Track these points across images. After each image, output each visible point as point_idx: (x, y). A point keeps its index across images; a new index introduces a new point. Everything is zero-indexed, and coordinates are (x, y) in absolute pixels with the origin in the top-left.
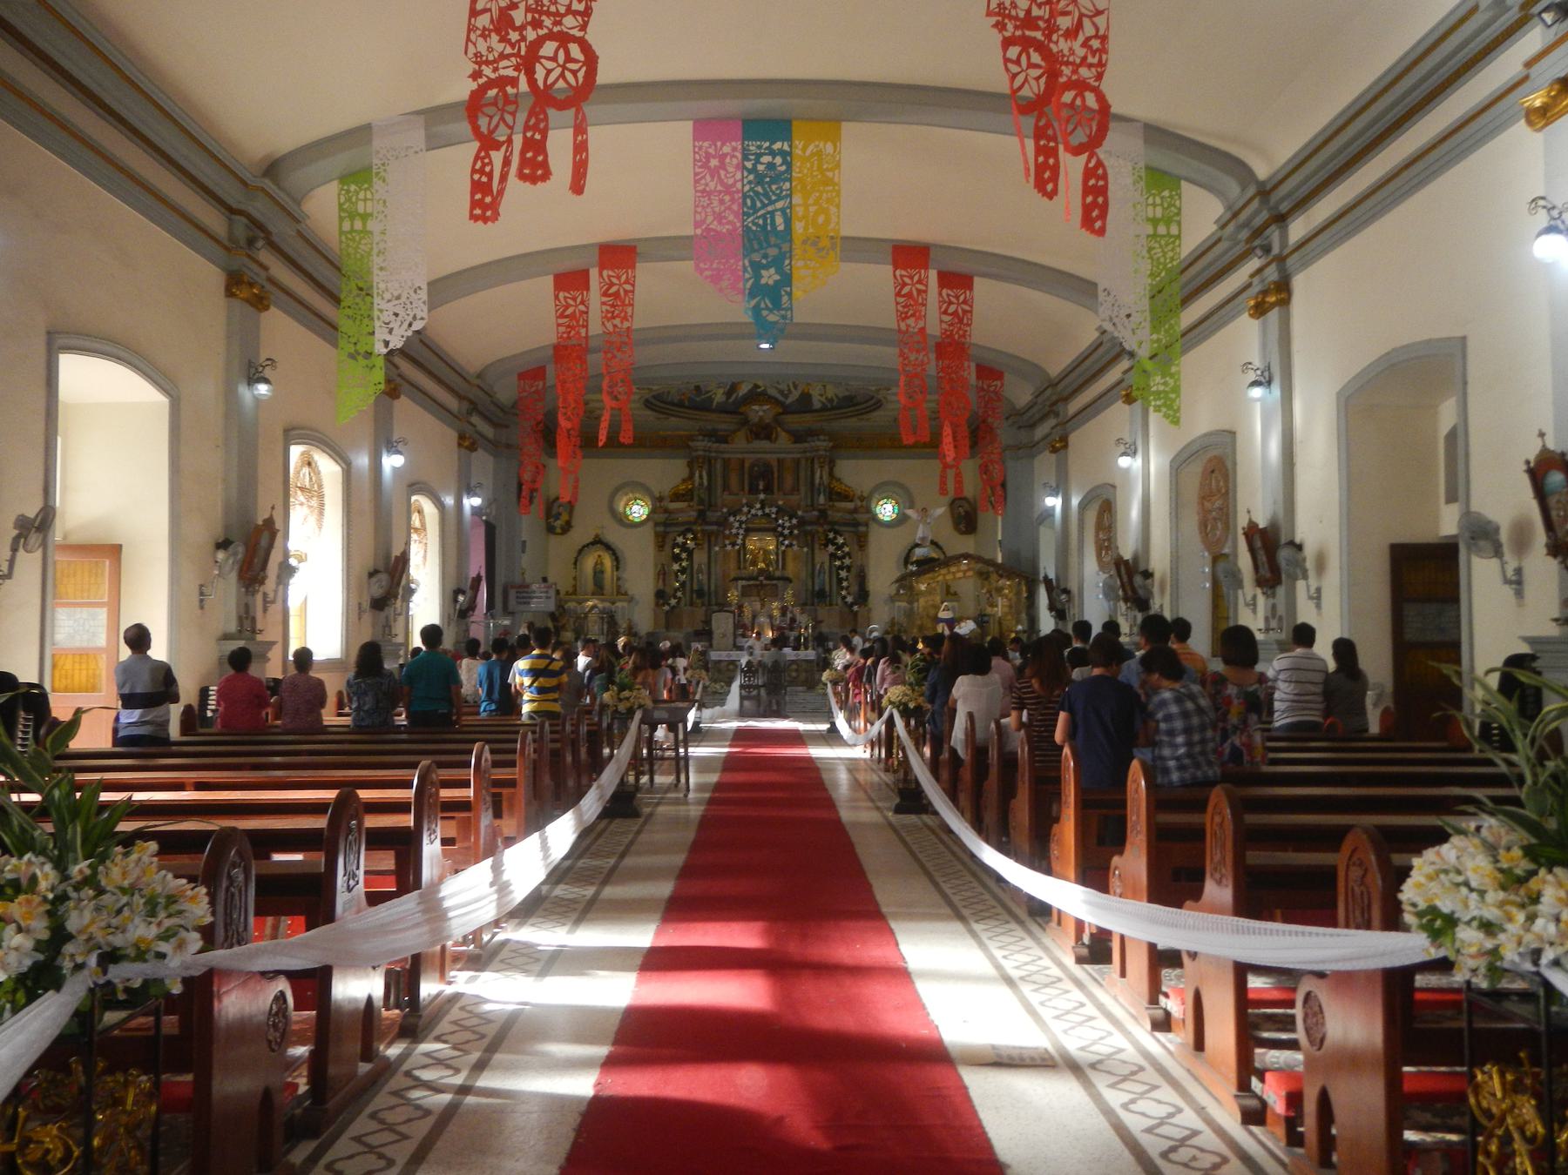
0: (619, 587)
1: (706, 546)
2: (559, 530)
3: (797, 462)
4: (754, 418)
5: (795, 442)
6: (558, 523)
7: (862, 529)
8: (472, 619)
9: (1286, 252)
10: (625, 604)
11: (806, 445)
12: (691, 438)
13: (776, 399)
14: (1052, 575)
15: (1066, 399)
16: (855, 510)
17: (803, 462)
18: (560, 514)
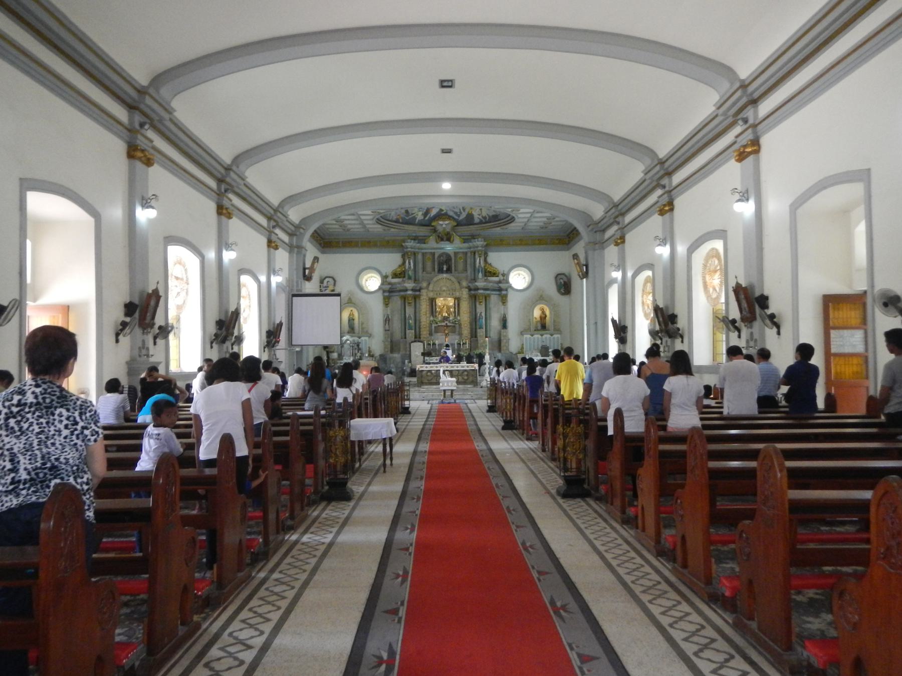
0: (363, 329)
1: (413, 304)
3: (466, 253)
5: (464, 243)
7: (504, 292)
8: (278, 348)
9: (757, 122)
10: (367, 338)
11: (471, 244)
12: (404, 242)
13: (453, 218)
14: (616, 318)
15: (623, 214)
16: (500, 282)
17: (469, 254)
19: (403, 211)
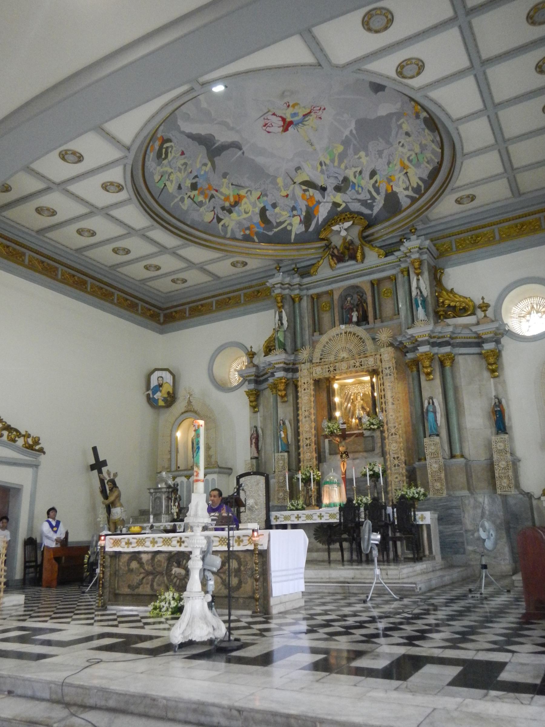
1: (291, 398)
2: (161, 403)
4: (337, 241)
5: (386, 256)
6: (158, 395)
13: (360, 213)
18: (160, 386)
19: (257, 219)
